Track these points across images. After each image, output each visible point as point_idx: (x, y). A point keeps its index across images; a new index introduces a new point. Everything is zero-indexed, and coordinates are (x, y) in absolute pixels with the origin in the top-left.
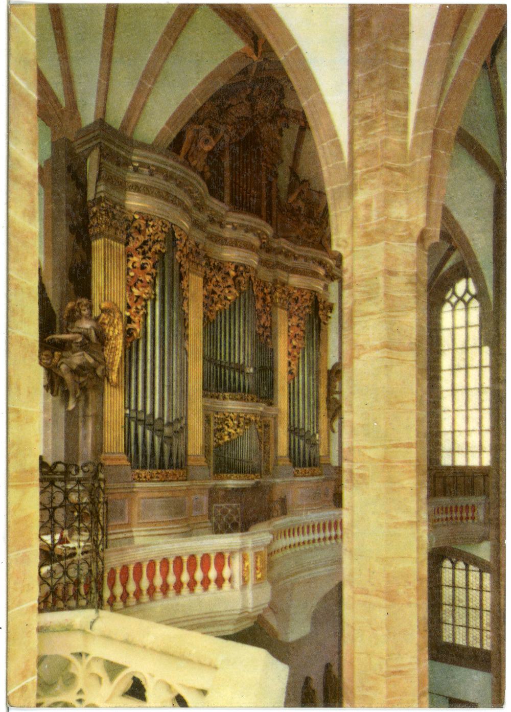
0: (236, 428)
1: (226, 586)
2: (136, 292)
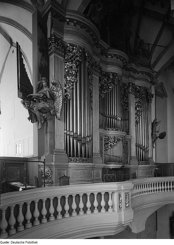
1: (110, 210)
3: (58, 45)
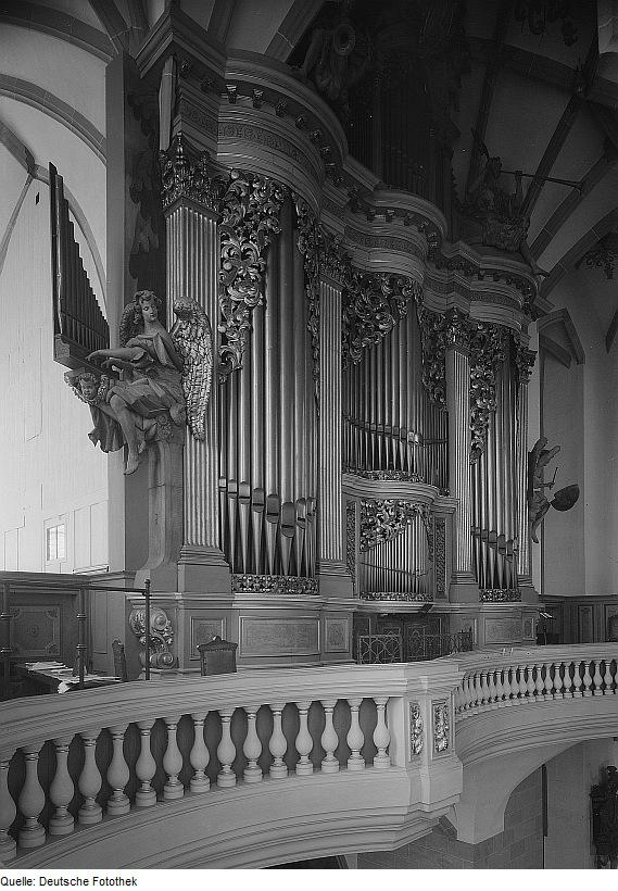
1: (380, 761)
3: (197, 176)
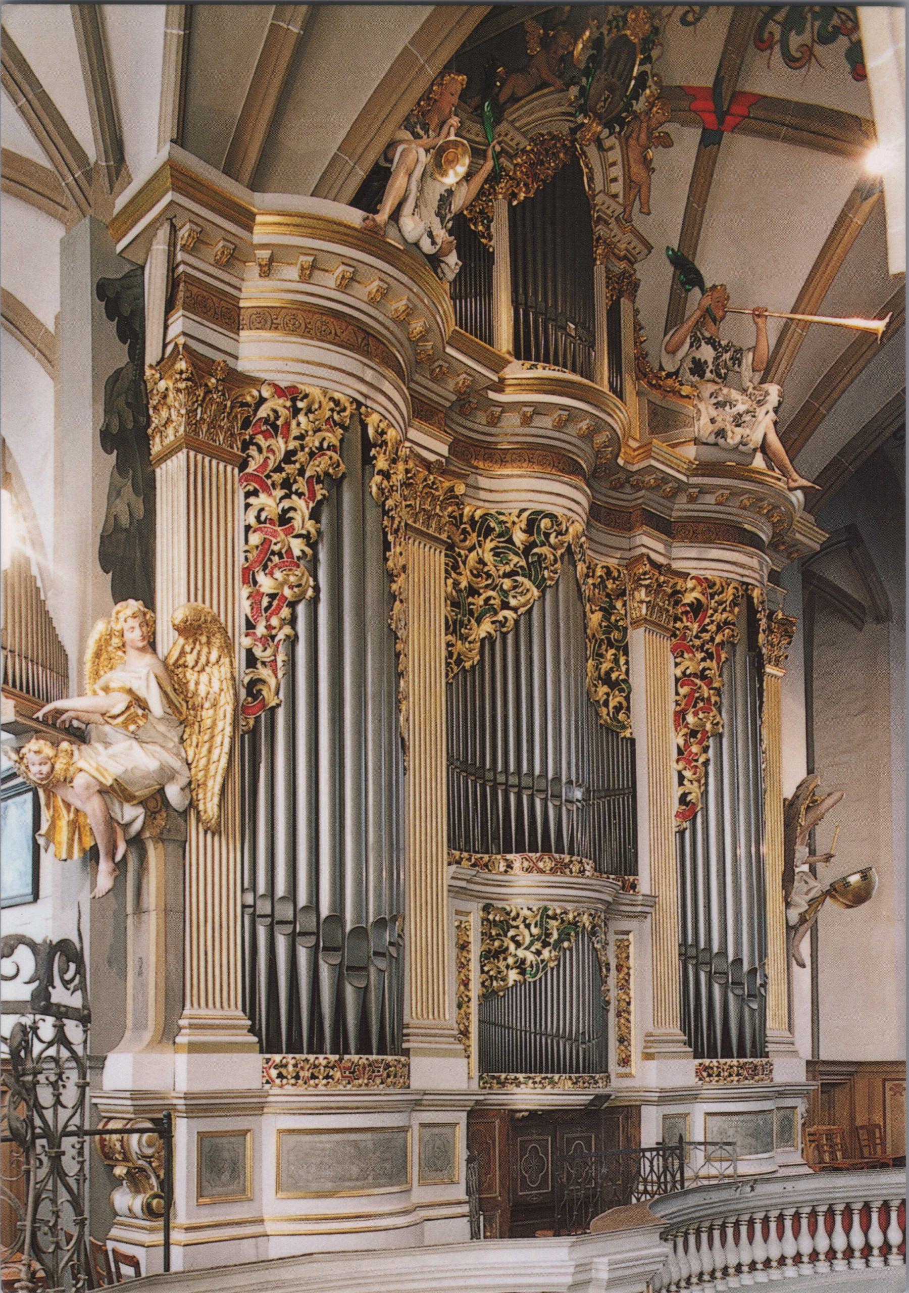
0: (538, 945)
2: (266, 584)
